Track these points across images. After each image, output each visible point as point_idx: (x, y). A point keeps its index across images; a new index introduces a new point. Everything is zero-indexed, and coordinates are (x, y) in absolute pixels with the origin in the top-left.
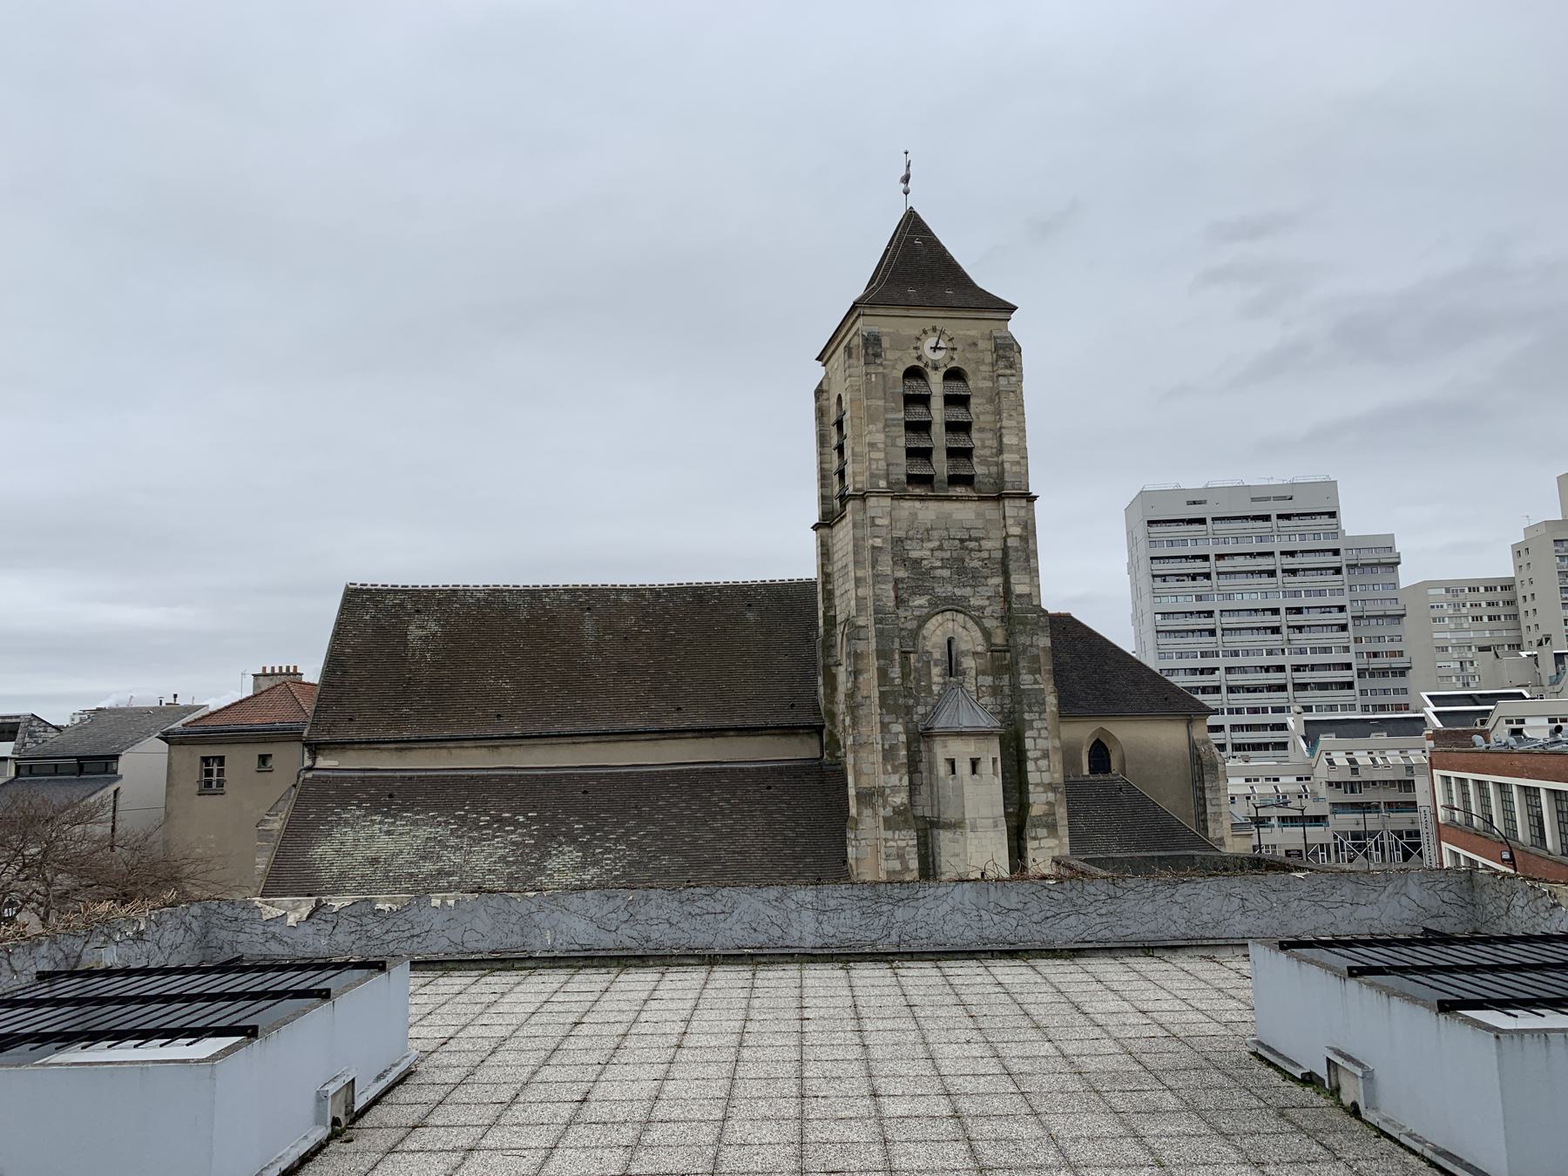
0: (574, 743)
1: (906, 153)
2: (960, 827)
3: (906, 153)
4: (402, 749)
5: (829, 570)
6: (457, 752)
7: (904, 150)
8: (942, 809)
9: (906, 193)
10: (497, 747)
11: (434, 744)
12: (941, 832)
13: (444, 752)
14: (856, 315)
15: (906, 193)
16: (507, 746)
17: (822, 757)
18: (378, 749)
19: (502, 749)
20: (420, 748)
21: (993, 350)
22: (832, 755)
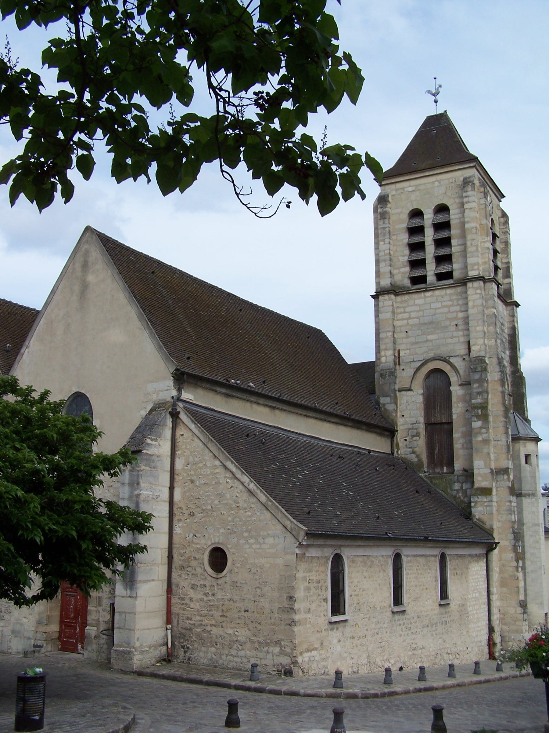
0: (307, 416)
1: (435, 78)
2: (534, 496)
3: (435, 78)
4: (227, 396)
5: (397, 323)
6: (255, 406)
7: (434, 77)
8: (523, 485)
9: (436, 102)
10: (273, 408)
11: (244, 396)
12: (523, 498)
13: (248, 405)
14: (472, 165)
15: (436, 102)
16: (278, 409)
17: (393, 453)
18: (216, 391)
19: (277, 412)
20: (237, 397)
21: (500, 216)
22: (397, 452)
